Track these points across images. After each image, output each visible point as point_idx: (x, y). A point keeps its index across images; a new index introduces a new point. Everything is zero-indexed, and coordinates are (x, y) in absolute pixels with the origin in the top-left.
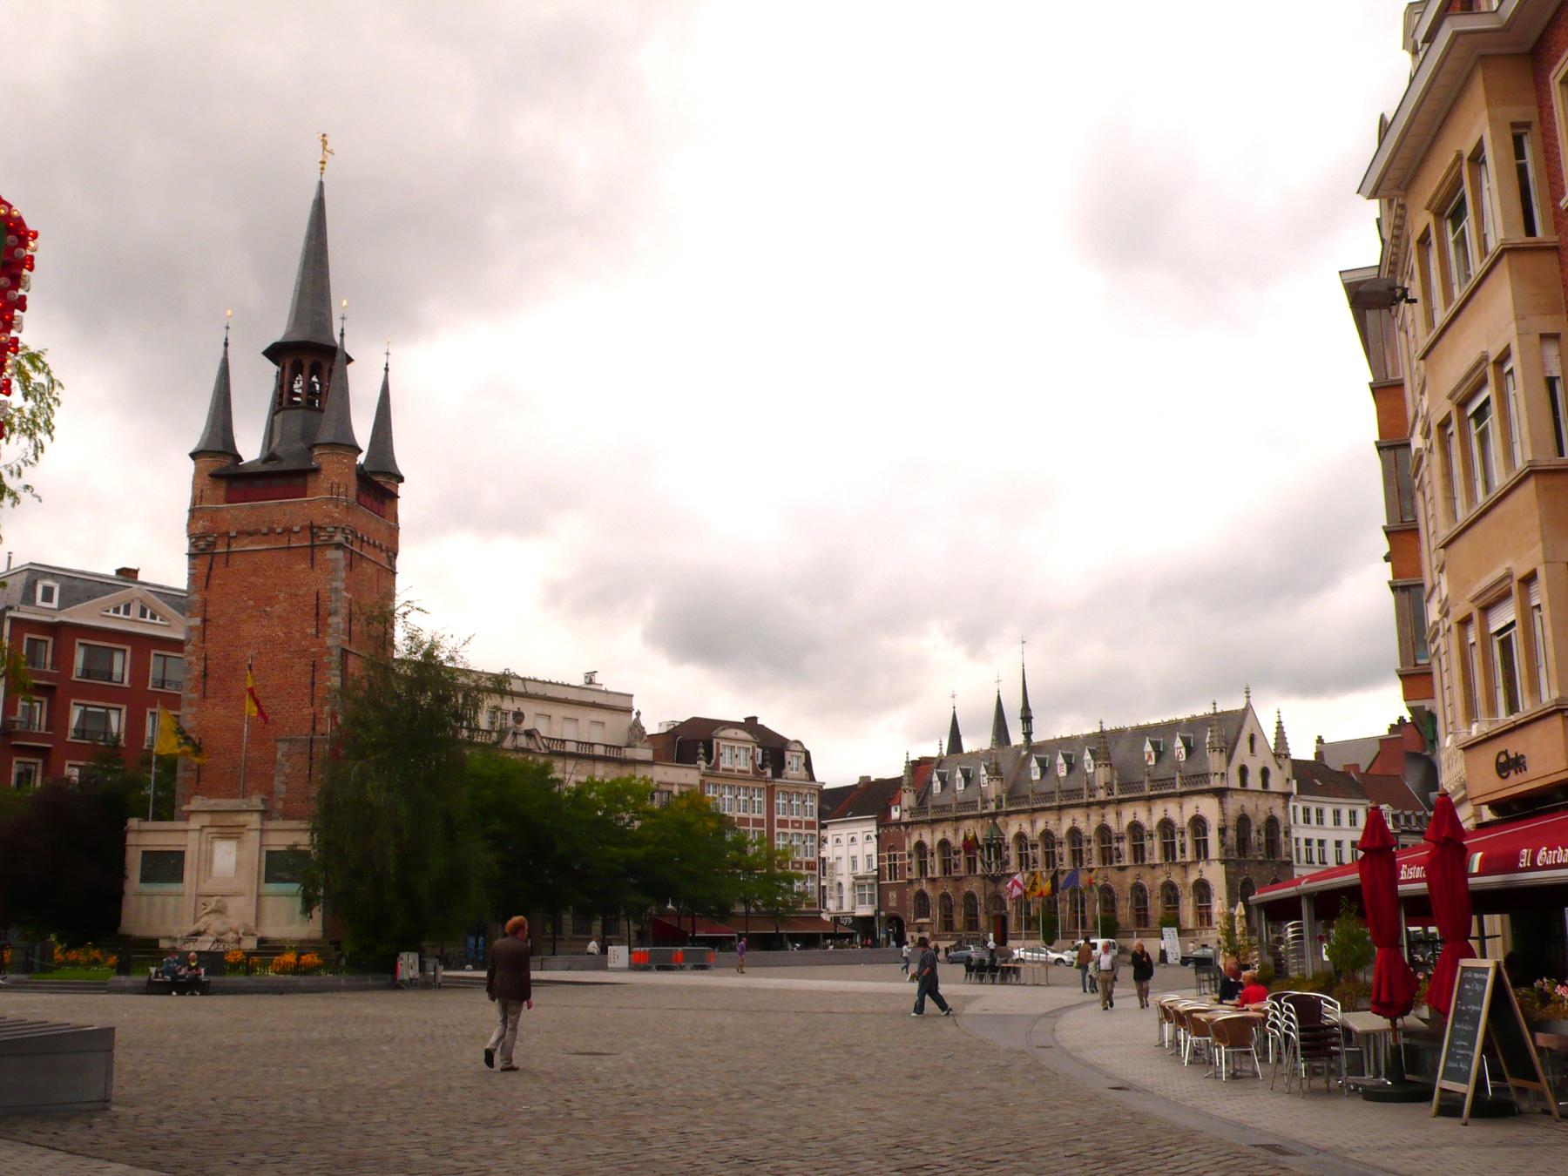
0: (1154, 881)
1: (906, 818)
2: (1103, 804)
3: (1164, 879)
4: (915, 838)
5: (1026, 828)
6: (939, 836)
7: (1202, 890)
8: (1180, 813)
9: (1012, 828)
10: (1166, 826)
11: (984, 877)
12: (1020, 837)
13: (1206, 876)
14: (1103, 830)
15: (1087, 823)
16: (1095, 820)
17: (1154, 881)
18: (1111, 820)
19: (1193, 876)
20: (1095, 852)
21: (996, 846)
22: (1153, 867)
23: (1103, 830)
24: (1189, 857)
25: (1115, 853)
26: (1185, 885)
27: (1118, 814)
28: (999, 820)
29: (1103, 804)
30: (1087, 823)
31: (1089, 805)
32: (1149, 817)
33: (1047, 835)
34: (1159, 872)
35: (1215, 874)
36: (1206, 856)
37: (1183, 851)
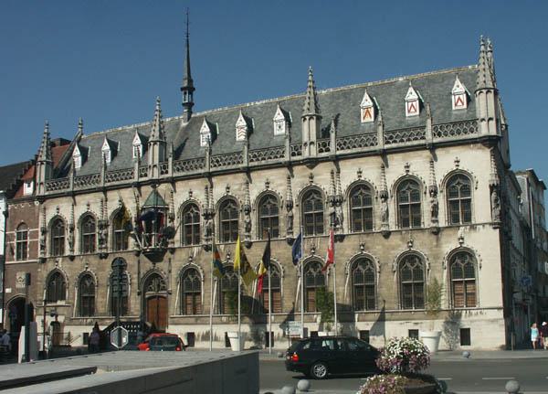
0: (386, 252)
1: (42, 191)
2: (312, 163)
3: (404, 248)
4: (51, 213)
5: (200, 196)
6: (81, 210)
7: (463, 263)
8: (430, 171)
9: (181, 196)
10: (408, 185)
11: (138, 254)
12: (189, 207)
13: (468, 244)
14: (311, 195)
15: (285, 186)
16: (301, 179)
17: (386, 252)
18: (323, 178)
19: (449, 245)
20: (297, 220)
21: (153, 219)
22: (387, 235)
23: (311, 195)
24: (443, 220)
25: (328, 219)
26: (436, 257)
27: (336, 173)
28: (162, 188)
29: (312, 163)
30: (285, 186)
31: (290, 165)
32: (381, 176)
33: (227, 203)
34: (394, 240)
35: (485, 244)
36: (468, 218)
37: (435, 213)
